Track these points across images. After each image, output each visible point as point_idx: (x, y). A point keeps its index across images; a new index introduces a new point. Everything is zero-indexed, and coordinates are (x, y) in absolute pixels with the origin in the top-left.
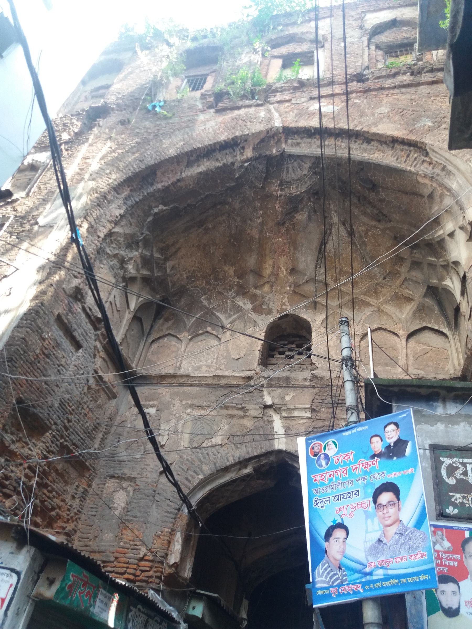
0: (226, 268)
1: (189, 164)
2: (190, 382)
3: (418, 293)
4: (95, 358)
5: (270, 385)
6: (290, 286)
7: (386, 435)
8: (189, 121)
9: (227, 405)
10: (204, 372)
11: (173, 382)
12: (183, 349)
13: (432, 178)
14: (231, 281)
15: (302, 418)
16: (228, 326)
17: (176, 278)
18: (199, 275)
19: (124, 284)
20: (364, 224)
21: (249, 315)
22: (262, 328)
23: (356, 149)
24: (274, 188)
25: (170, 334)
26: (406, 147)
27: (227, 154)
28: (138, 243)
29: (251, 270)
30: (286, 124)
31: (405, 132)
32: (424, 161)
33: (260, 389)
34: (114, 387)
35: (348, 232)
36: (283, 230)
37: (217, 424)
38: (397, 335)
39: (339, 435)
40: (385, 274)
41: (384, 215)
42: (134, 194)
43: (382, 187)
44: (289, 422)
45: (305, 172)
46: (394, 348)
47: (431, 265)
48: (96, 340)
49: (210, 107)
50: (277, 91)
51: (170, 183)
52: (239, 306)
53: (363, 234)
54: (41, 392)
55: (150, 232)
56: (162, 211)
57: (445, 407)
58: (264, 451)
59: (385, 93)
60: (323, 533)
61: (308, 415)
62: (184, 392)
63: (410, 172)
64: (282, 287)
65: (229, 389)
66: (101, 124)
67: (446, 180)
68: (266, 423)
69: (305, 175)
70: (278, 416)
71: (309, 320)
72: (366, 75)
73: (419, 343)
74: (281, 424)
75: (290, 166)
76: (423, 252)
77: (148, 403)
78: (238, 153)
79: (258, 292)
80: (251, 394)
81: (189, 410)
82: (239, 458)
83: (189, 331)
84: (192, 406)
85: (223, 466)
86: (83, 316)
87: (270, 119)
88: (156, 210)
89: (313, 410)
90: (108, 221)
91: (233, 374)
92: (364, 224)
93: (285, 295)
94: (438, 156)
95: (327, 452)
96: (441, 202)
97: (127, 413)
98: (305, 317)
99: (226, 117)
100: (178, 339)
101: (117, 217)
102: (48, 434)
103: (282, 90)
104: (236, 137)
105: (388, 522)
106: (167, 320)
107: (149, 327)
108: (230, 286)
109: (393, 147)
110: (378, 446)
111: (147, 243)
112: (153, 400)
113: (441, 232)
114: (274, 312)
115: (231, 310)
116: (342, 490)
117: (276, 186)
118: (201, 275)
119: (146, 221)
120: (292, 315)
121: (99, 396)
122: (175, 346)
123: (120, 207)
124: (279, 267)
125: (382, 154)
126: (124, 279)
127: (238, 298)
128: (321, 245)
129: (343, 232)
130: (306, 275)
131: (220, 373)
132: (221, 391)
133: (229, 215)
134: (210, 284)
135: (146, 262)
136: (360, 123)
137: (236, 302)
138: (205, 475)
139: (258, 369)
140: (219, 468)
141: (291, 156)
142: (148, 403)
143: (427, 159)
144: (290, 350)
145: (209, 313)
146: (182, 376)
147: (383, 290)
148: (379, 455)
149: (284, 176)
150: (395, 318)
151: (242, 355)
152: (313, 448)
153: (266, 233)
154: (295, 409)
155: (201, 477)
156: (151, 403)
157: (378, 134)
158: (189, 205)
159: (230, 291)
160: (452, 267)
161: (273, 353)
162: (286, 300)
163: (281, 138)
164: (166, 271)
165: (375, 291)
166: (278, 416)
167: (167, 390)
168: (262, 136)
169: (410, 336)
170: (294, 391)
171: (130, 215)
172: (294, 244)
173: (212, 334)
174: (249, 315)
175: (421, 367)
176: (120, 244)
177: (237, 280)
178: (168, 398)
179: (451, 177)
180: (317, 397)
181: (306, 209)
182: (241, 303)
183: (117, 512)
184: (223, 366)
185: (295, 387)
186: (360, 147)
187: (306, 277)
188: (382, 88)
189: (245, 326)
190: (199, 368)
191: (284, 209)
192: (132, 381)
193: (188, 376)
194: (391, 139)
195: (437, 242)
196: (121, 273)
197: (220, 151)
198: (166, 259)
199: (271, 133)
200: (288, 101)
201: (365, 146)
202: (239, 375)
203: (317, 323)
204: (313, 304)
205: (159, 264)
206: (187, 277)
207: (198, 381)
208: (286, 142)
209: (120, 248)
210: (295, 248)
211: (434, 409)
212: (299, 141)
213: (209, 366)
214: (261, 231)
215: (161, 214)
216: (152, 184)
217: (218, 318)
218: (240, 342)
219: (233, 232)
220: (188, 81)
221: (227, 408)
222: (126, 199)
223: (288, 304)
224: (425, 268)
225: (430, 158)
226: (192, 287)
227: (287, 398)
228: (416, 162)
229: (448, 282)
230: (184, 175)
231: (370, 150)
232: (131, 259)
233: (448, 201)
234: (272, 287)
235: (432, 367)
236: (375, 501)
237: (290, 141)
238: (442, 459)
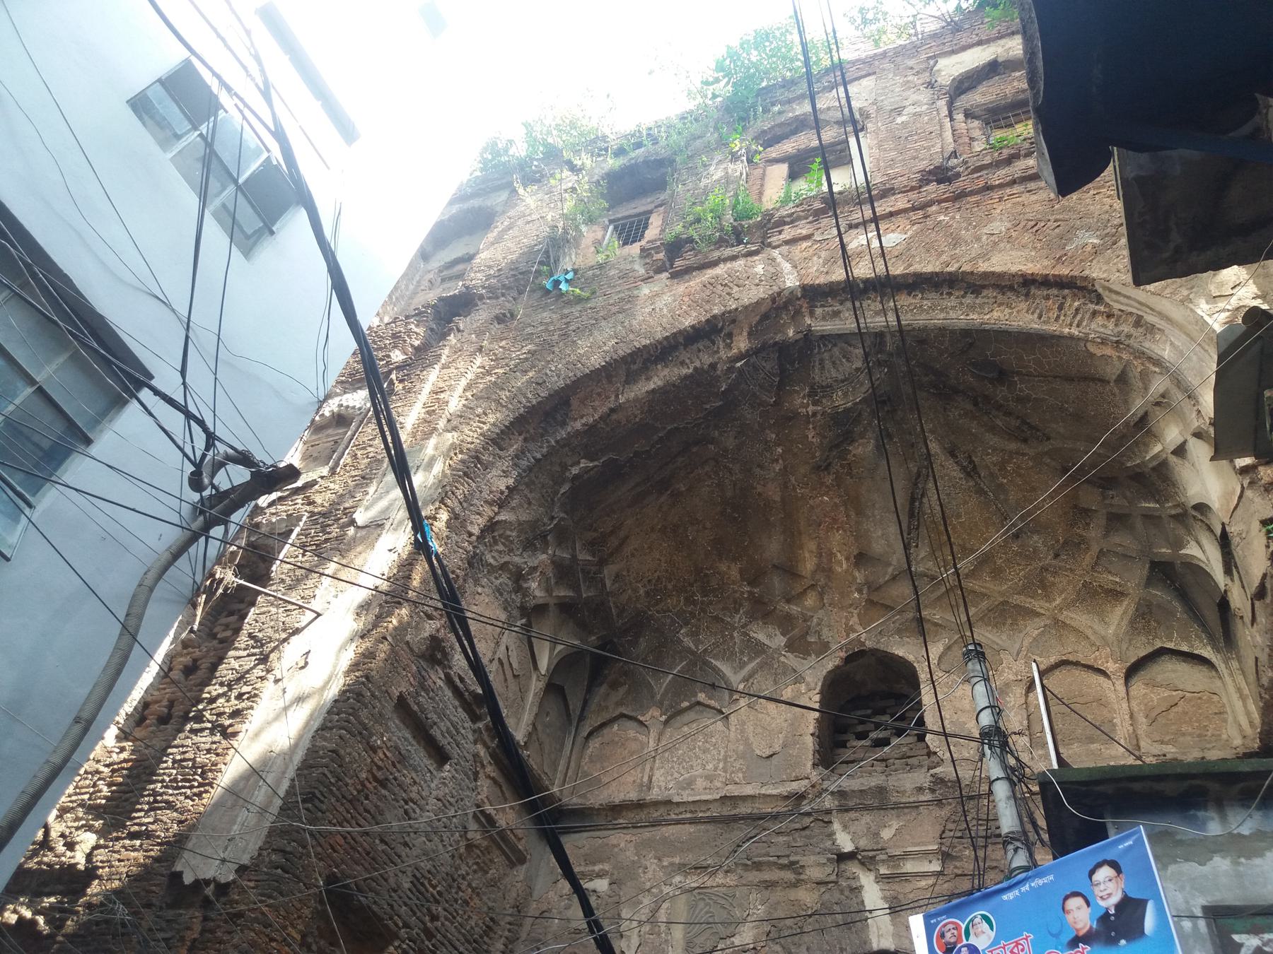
0: (723, 567)
1: (631, 378)
2: (674, 816)
3: (1133, 579)
4: (476, 780)
5: (844, 810)
6: (860, 591)
7: (1096, 890)
8: (622, 299)
9: (756, 859)
10: (702, 792)
12: (652, 744)
13: (1117, 342)
14: (735, 592)
15: (924, 875)
16: (741, 687)
17: (624, 597)
18: (670, 587)
19: (524, 621)
20: (994, 450)
21: (782, 659)
22: (813, 685)
23: (953, 308)
24: (800, 401)
25: (623, 716)
26: (1055, 291)
27: (699, 351)
28: (545, 536)
29: (774, 566)
30: (808, 281)
31: (1046, 262)
32: (1094, 313)
33: (823, 818)
34: (520, 839)
35: (963, 469)
36: (829, 480)
37: (740, 905)
38: (1103, 673)
39: (994, 902)
40: (1057, 547)
41: (1031, 427)
42: (531, 446)
43: (1018, 373)
44: (896, 887)
45: (858, 364)
46: (1101, 702)
47: (1149, 517)
48: (475, 742)
49: (659, 270)
50: (785, 223)
51: (596, 417)
52: (759, 643)
53: (995, 469)
54: (373, 859)
55: (566, 512)
56: (587, 470)
57: (1224, 819)
59: (996, 195)
61: (936, 867)
62: (664, 840)
63: (1071, 337)
66: (461, 326)
67: (1147, 344)
68: (847, 893)
69: (857, 369)
70: (872, 876)
71: (911, 658)
72: (953, 168)
73: (1152, 684)
74: (880, 894)
75: (826, 356)
76: (1128, 494)
77: (591, 868)
78: (722, 345)
79: (794, 609)
80: (807, 832)
81: (677, 879)
83: (660, 705)
84: (682, 869)
86: (448, 693)
87: (776, 276)
88: (575, 470)
89: (946, 857)
90: (486, 502)
91: (763, 792)
92: (994, 450)
93: (851, 610)
94: (1121, 299)
95: (973, 940)
96: (1146, 389)
97: (551, 894)
98: (900, 652)
100: (641, 723)
101: (502, 493)
102: (391, 949)
103: (792, 220)
104: (714, 317)
106: (614, 686)
107: (579, 705)
108: (735, 602)
109: (1027, 295)
110: (1081, 917)
111: (562, 536)
112: (601, 861)
113: (1157, 448)
115: (742, 653)
117: (804, 398)
118: (675, 586)
119: (556, 493)
120: (874, 652)
121: (491, 861)
122: (636, 739)
123: (506, 474)
124: (831, 555)
125: (1007, 311)
126: (524, 611)
127: (754, 627)
128: (913, 500)
129: (956, 473)
130: (890, 565)
131: (734, 791)
133: (717, 462)
134: (694, 603)
135: (564, 572)
136: (953, 257)
137: (752, 634)
139: (815, 776)
141: (826, 338)
142: (591, 868)
143: (1102, 308)
144: (877, 726)
145: (698, 661)
146: (656, 804)
147: (1057, 580)
148: (1087, 938)
149: (817, 376)
150: (1092, 638)
151: (777, 748)
152: (942, 935)
153: (794, 489)
154: (906, 856)
156: (597, 868)
157: (993, 273)
158: (636, 454)
159: (737, 611)
160: (1194, 517)
161: (845, 737)
162: (854, 620)
163: (801, 307)
164: (604, 585)
165: (1040, 584)
166: (872, 876)
167: (628, 838)
168: (763, 309)
169: (1132, 672)
170: (898, 817)
171: (527, 485)
172: (855, 504)
173: (708, 706)
174: (782, 659)
175: (1167, 738)
176: (512, 542)
177: (747, 589)
178: (630, 855)
179: (1158, 337)
181: (869, 434)
182: (761, 637)
184: (740, 775)
185: (898, 807)
186: (961, 303)
187: (890, 570)
188: (988, 188)
190: (689, 784)
191: (825, 437)
192: (554, 822)
193: (668, 803)
194: (1021, 280)
195: (1154, 469)
196: (517, 598)
197: (686, 346)
198: (602, 562)
199: (780, 302)
201: (969, 299)
202: (775, 792)
204: (914, 624)
205: (589, 573)
206: (647, 593)
207: (691, 812)
208: (812, 314)
209: (511, 550)
210: (859, 513)
211: (1202, 826)
212: (838, 307)
214: (785, 486)
215: (586, 476)
216: (563, 424)
217: (717, 671)
218: (768, 719)
219: (729, 494)
220: (616, 228)
221: (758, 866)
222: (517, 456)
224: (1139, 524)
225: (1107, 305)
227: (886, 834)
228: (1078, 318)
229: (1192, 550)
230: (622, 400)
231: (981, 306)
232: (534, 569)
233: (1159, 385)
234: (821, 595)
237: (819, 311)
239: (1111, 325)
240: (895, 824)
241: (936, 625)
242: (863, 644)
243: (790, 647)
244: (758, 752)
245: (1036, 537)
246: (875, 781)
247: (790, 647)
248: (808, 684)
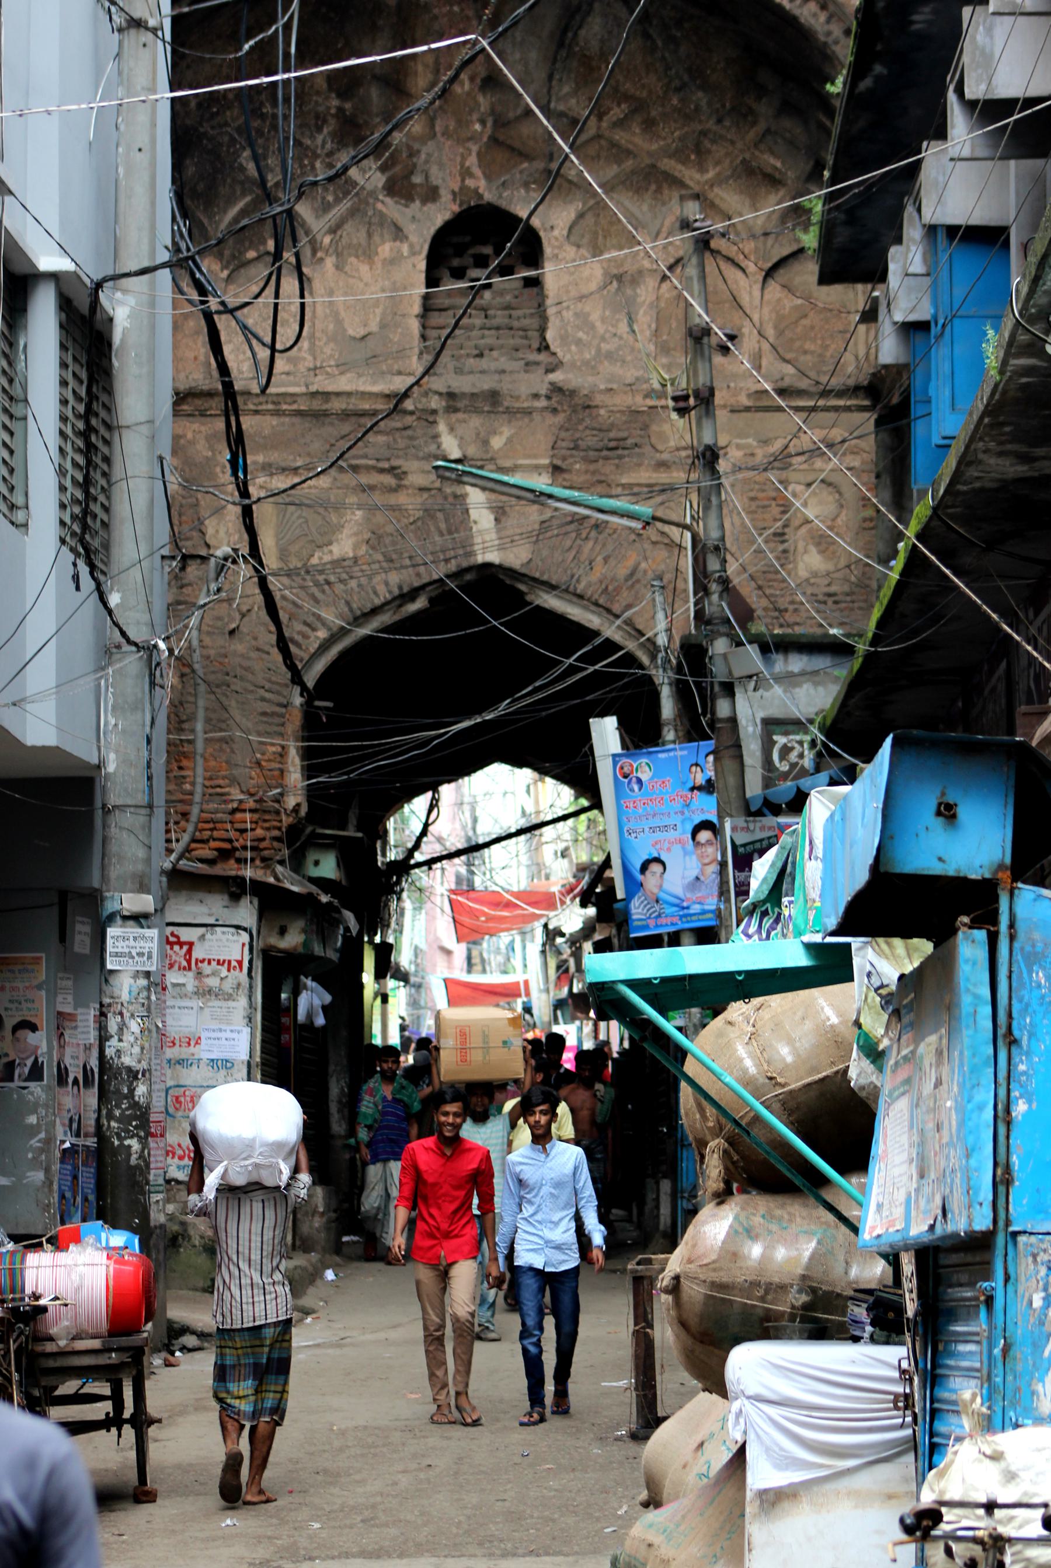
2: (252, 407)
5: (451, 409)
6: (483, 122)
11: (206, 405)
33: (429, 417)
38: (743, 270)
39: (653, 756)
57: (786, 660)
60: (638, 866)
64: (459, 122)
65: (353, 419)
68: (451, 499)
80: (409, 432)
82: (400, 588)
85: (368, 607)
95: (639, 775)
105: (707, 861)
108: (317, 117)
114: (445, 196)
116: (657, 822)
132: (332, 424)
138: (329, 629)
140: (359, 613)
147: (714, 148)
148: (700, 788)
151: (374, 327)
152: (622, 768)
159: (319, 129)
162: (472, 161)
165: (696, 150)
167: (196, 426)
174: (379, 206)
177: (335, 102)
180: (563, 434)
189: (370, 235)
202: (376, 389)
203: (556, 233)
207: (274, 403)
218: (361, 285)
223: (477, 171)
226: (213, 128)
227: (497, 443)
234: (432, 121)
235: (812, 353)
236: (694, 837)
238: (775, 737)
239: (823, 17)
240: (507, 432)
241: (570, 182)
242: (480, 197)
243: (391, 189)
244: (351, 332)
245: (700, 94)
246: (486, 384)
247: (391, 189)
248: (411, 246)
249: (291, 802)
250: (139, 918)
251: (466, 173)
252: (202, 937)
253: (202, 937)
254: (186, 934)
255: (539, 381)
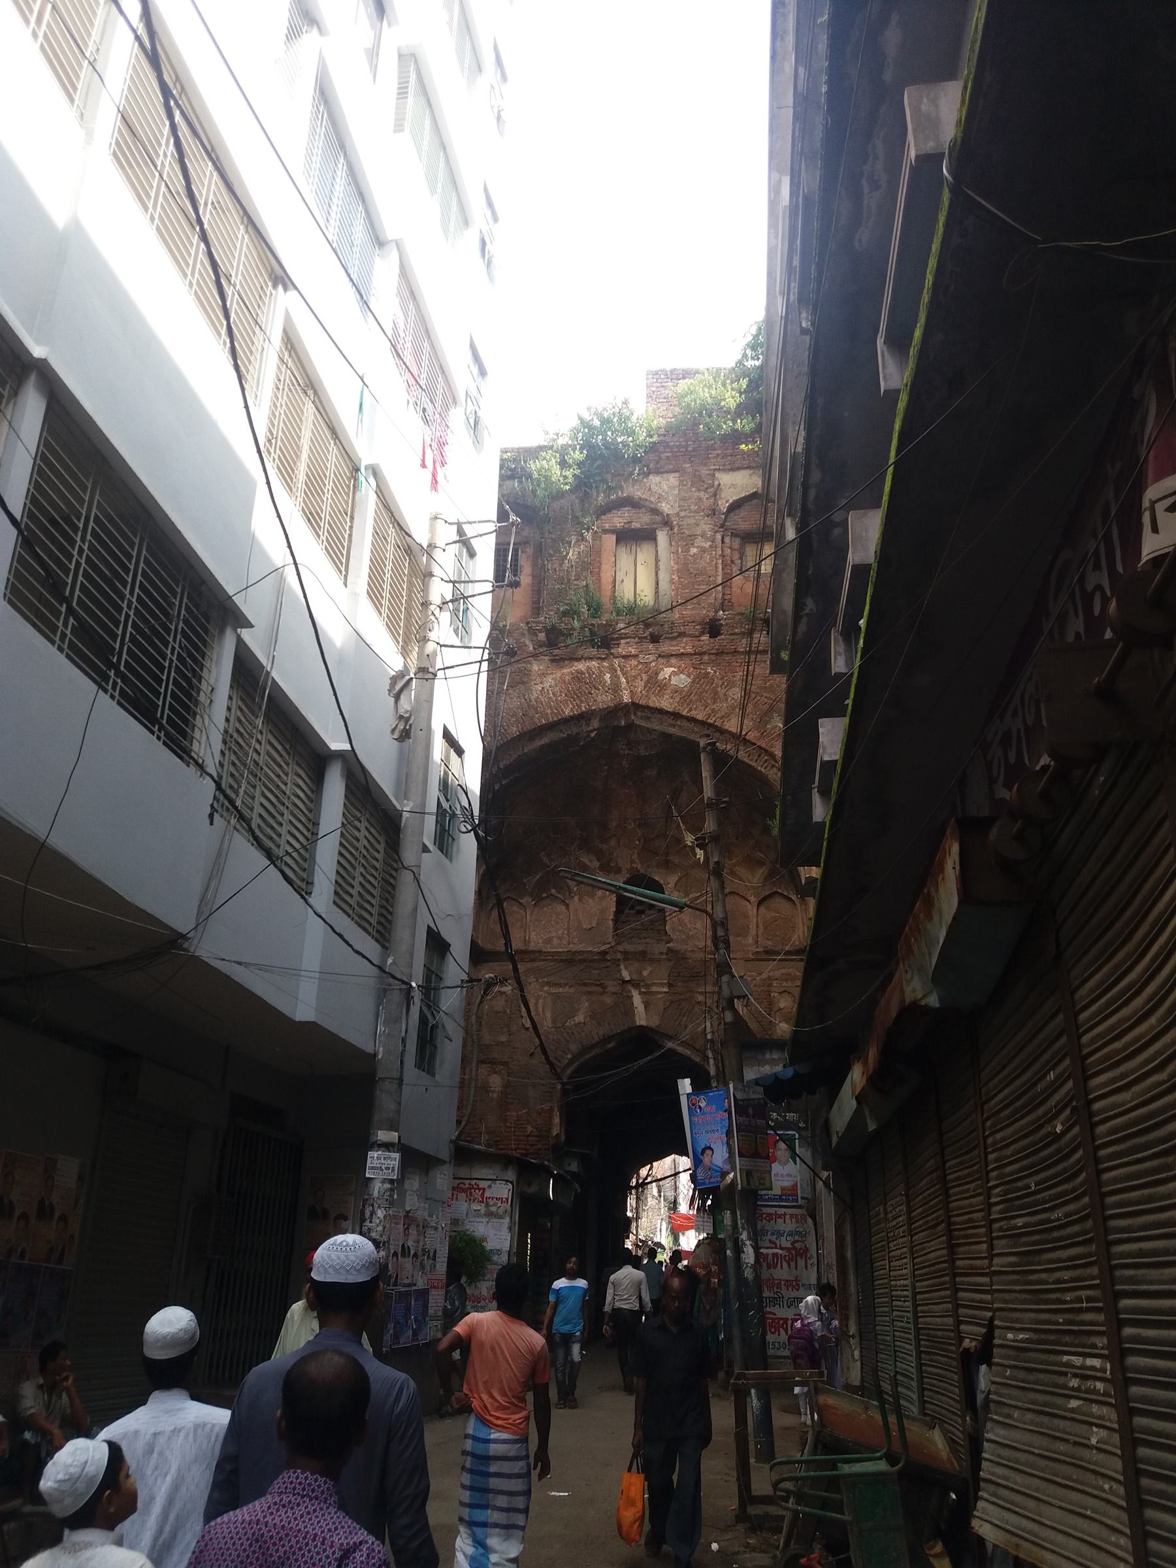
5: (626, 959)
10: (556, 946)
33: (616, 963)
46: (746, 916)
52: (584, 864)
58: (626, 1027)
71: (662, 882)
79: (605, 847)
81: (546, 988)
84: (548, 984)
87: (616, 688)
89: (670, 985)
98: (657, 878)
99: (565, 671)
114: (624, 871)
146: (534, 952)
151: (594, 925)
154: (653, 984)
155: (569, 1056)
162: (635, 856)
182: (586, 860)
183: (495, 1095)
185: (652, 961)
190: (549, 941)
193: (540, 952)
200: (636, 656)
213: (560, 939)
221: (585, 984)
227: (645, 973)
243: (602, 868)
246: (641, 948)
249: (555, 1132)
250: (387, 1146)
251: (633, 862)
252: (490, 1187)
253: (490, 1187)
254: (483, 1184)
255: (663, 948)
